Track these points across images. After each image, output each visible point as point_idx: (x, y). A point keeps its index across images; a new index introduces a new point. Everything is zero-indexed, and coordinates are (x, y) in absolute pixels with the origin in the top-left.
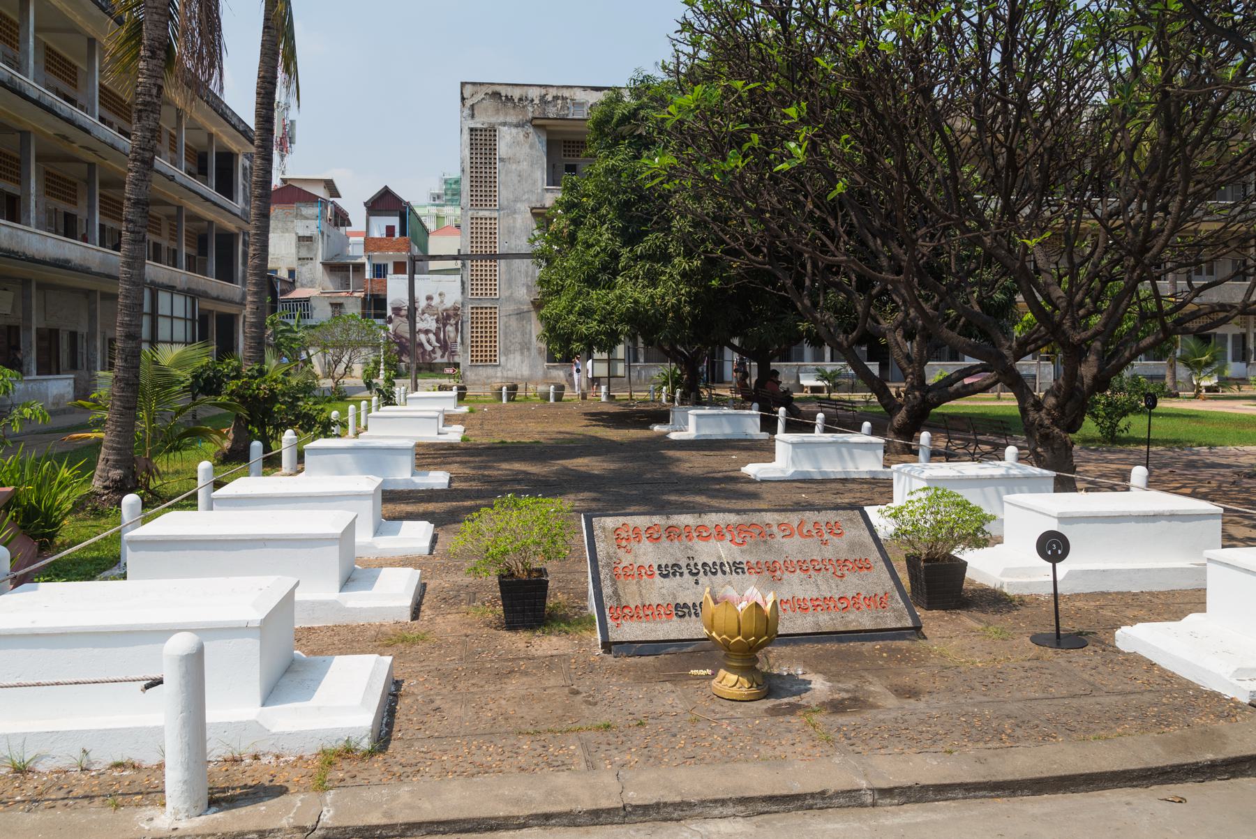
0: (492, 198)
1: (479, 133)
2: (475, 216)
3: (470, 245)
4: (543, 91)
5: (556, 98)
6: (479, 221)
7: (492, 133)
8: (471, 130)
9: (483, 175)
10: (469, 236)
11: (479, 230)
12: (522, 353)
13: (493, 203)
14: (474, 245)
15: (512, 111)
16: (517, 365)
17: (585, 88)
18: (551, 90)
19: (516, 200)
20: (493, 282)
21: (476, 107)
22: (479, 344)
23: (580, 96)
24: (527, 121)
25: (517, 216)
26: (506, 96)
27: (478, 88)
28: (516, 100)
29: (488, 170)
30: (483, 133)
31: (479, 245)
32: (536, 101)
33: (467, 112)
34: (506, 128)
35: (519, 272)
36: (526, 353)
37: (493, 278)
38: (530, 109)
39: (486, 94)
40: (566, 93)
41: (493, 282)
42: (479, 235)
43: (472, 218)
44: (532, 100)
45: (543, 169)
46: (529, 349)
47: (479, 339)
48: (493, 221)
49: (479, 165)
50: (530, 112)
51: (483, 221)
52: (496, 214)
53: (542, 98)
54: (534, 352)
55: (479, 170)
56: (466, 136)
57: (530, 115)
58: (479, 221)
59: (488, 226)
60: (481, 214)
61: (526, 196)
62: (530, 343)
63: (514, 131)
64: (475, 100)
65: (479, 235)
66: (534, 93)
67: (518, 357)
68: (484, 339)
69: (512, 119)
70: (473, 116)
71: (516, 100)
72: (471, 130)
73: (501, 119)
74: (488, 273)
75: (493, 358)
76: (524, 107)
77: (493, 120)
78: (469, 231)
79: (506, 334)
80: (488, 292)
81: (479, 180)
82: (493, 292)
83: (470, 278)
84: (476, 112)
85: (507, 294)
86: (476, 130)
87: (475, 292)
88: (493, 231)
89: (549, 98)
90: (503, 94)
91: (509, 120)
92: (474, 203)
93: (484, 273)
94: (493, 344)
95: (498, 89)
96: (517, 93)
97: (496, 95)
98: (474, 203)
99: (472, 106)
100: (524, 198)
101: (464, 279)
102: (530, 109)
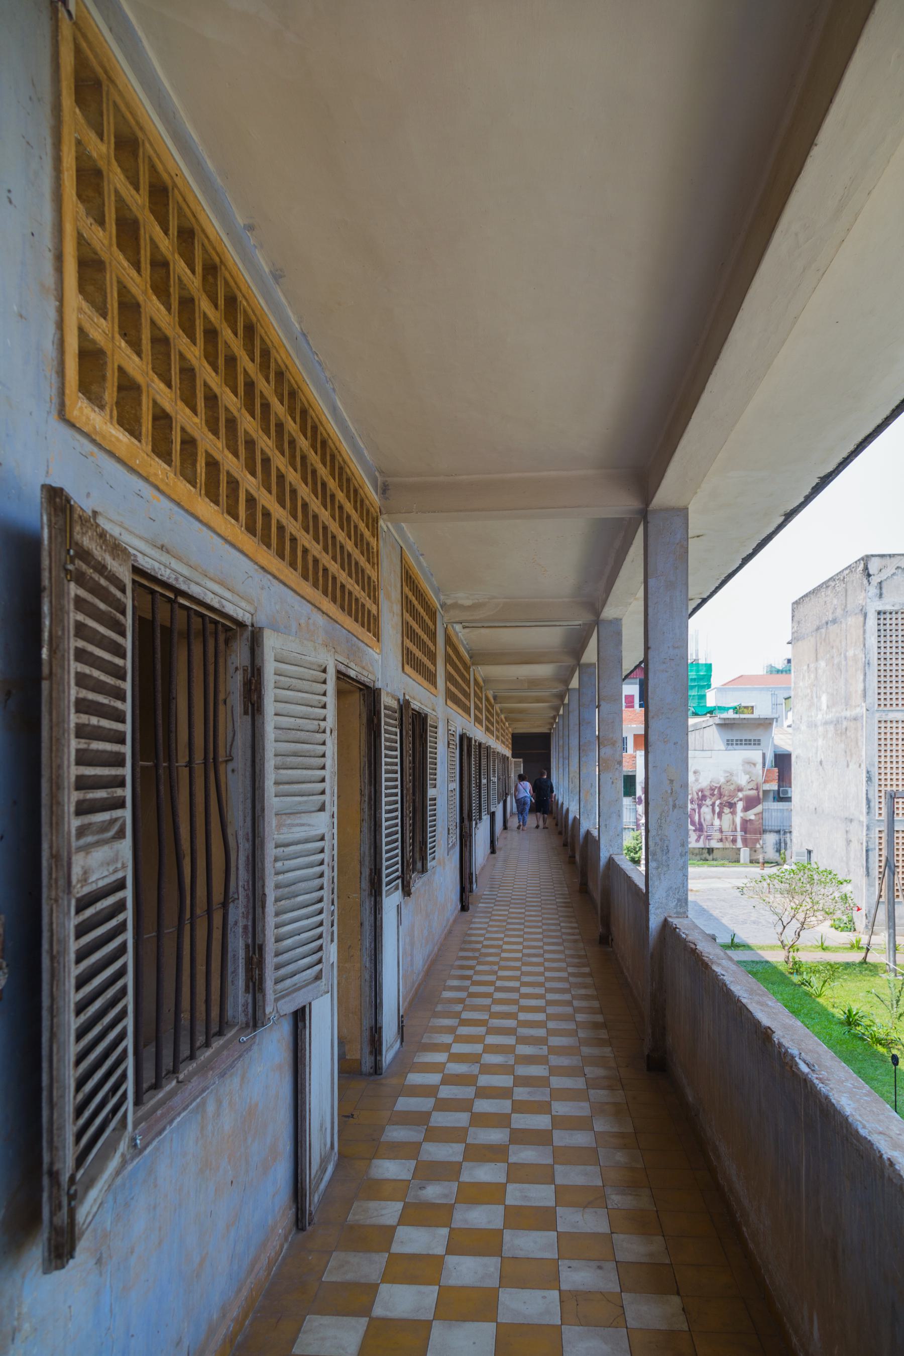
2: (883, 719)
3: (877, 754)
6: (889, 725)
8: (879, 613)
10: (877, 742)
11: (888, 736)
14: (883, 754)
21: (884, 585)
27: (887, 561)
30: (894, 616)
31: (888, 754)
39: (898, 568)
42: (889, 742)
43: (880, 722)
49: (888, 656)
51: (894, 725)
55: (888, 662)
58: (889, 725)
60: (891, 716)
64: (883, 576)
65: (889, 742)
70: (881, 595)
72: (879, 613)
78: (876, 737)
81: (888, 674)
83: (877, 794)
84: (884, 591)
86: (885, 613)
92: (882, 702)
98: (882, 702)
99: (880, 583)
101: (870, 796)
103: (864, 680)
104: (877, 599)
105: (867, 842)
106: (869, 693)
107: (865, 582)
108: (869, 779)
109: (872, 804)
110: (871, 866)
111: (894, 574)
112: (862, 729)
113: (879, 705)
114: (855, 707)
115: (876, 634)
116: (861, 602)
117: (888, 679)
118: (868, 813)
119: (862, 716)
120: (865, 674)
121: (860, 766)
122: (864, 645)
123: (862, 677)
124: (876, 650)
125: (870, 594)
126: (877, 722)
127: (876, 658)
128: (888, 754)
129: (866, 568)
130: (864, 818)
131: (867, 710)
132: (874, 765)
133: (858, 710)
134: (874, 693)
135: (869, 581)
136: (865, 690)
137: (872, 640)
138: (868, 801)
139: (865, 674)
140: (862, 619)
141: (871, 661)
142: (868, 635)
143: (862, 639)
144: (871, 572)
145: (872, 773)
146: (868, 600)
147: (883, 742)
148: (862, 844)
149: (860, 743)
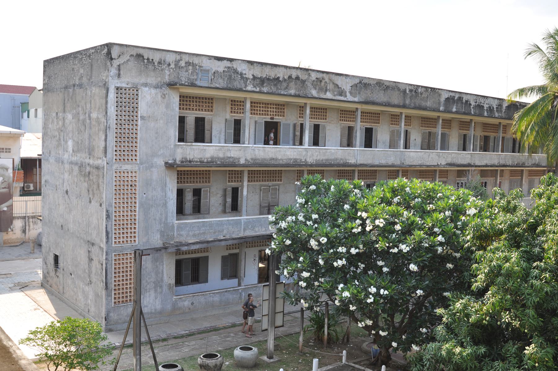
0: (134, 153)
4: (178, 57)
5: (188, 64)
9: (127, 131)
12: (156, 291)
13: (134, 158)
15: (152, 74)
16: (151, 301)
17: (210, 57)
18: (184, 56)
19: (154, 155)
20: (133, 230)
21: (122, 67)
22: (121, 287)
23: (206, 64)
25: (153, 169)
26: (148, 59)
27: (125, 49)
28: (156, 64)
29: (131, 127)
32: (173, 66)
34: (147, 89)
35: (155, 219)
36: (159, 290)
37: (133, 226)
38: (167, 72)
39: (132, 55)
40: (196, 61)
41: (133, 230)
42: (122, 187)
44: (169, 65)
46: (161, 287)
47: (121, 283)
48: (134, 174)
51: (126, 175)
52: (136, 168)
53: (177, 63)
54: (165, 288)
57: (167, 79)
58: (122, 174)
59: (130, 179)
61: (162, 152)
62: (162, 280)
63: (153, 91)
65: (122, 187)
66: (171, 58)
68: (125, 282)
69: (152, 80)
70: (119, 75)
73: (143, 80)
74: (129, 222)
76: (162, 70)
77: (136, 80)
80: (129, 239)
82: (133, 239)
84: (122, 72)
85: (144, 240)
87: (117, 240)
88: (133, 184)
89: (183, 64)
90: (146, 57)
93: (125, 222)
95: (141, 51)
96: (156, 57)
97: (139, 56)
98: (118, 157)
99: (119, 66)
100: (160, 153)
101: (109, 230)
102: (167, 72)
103: (106, 140)
104: (116, 78)
105: (106, 264)
106: (109, 150)
107: (109, 64)
108: (108, 217)
109: (110, 236)
110: (109, 281)
111: (128, 60)
112: (103, 177)
114: (98, 158)
116: (104, 78)
117: (123, 140)
118: (107, 242)
119: (104, 167)
120: (106, 136)
121: (101, 205)
122: (106, 113)
123: (103, 137)
124: (115, 117)
125: (111, 74)
128: (122, 196)
129: (109, 53)
130: (103, 245)
131: (107, 163)
132: (111, 206)
133: (100, 162)
134: (113, 150)
135: (111, 63)
136: (106, 148)
137: (112, 110)
138: (107, 233)
139: (106, 136)
140: (105, 92)
141: (111, 126)
142: (109, 105)
143: (104, 107)
144: (113, 57)
145: (110, 212)
146: (110, 78)
148: (102, 265)
149: (101, 188)
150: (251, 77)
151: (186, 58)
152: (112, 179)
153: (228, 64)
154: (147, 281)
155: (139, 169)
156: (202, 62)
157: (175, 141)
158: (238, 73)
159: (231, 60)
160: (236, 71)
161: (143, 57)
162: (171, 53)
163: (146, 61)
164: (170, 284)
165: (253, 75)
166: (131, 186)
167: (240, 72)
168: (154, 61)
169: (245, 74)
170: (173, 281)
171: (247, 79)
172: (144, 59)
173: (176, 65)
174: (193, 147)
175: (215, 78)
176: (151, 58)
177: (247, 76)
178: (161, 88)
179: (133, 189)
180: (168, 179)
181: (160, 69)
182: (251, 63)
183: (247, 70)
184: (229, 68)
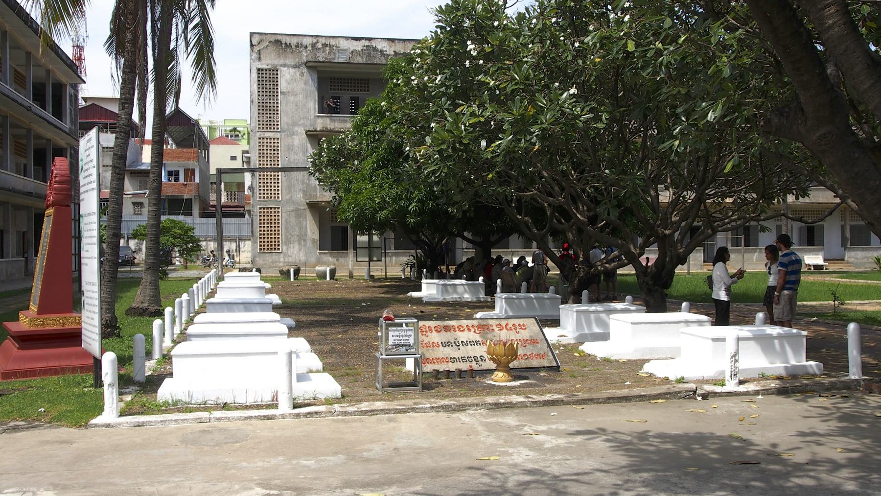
1: (264, 72)
4: (315, 40)
6: (265, 141)
7: (275, 73)
8: (259, 70)
12: (300, 243)
14: (261, 159)
18: (320, 39)
24: (302, 64)
26: (286, 44)
28: (294, 47)
31: (265, 159)
32: (310, 48)
33: (255, 55)
43: (260, 139)
44: (306, 47)
45: (315, 100)
46: (305, 240)
48: (276, 141)
50: (305, 56)
52: (278, 136)
54: (309, 243)
56: (255, 75)
58: (265, 141)
60: (267, 135)
63: (292, 70)
66: (307, 41)
67: (297, 247)
69: (290, 61)
71: (294, 47)
72: (259, 70)
73: (282, 62)
75: (277, 247)
76: (299, 52)
77: (276, 62)
78: (257, 148)
79: (286, 229)
91: (288, 62)
94: (277, 236)
95: (279, 38)
96: (294, 41)
97: (278, 42)
98: (261, 126)
99: (259, 51)
109: (255, 191)
111: (267, 46)
113: (259, 128)
115: (257, 83)
126: (257, 139)
127: (257, 99)
144: (253, 44)
147: (261, 152)
150: (393, 53)
151: (323, 41)
152: (256, 144)
153: (367, 43)
154: (291, 234)
155: (281, 136)
156: (339, 43)
157: (315, 113)
158: (377, 51)
159: (370, 39)
160: (375, 49)
161: (281, 42)
162: (307, 38)
163: (284, 45)
164: (314, 239)
165: (394, 52)
166: (274, 150)
167: (379, 50)
168: (292, 45)
169: (386, 51)
170: (316, 236)
171: (388, 55)
172: (282, 44)
173: (312, 47)
174: (334, 118)
175: (354, 57)
176: (288, 43)
177: (388, 53)
178: (299, 67)
179: (276, 152)
180: (309, 146)
181: (297, 51)
182: (392, 40)
183: (388, 47)
184: (367, 46)
